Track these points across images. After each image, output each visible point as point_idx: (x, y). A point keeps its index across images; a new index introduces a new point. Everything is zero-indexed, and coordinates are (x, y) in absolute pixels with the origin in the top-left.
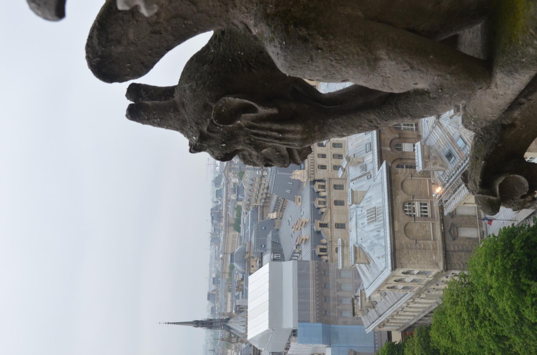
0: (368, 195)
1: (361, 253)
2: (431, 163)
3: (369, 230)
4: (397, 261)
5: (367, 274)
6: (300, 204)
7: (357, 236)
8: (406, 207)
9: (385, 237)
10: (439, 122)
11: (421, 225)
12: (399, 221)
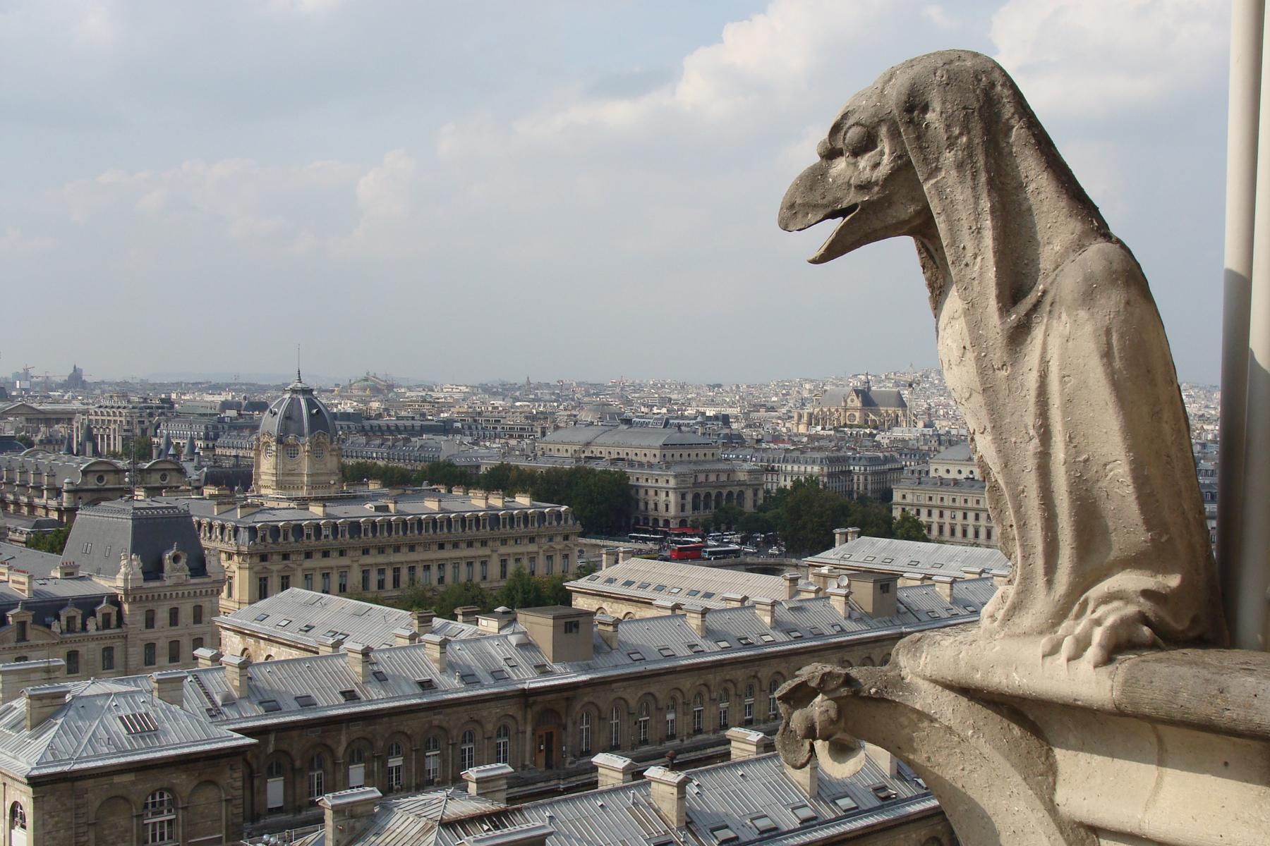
9: (98, 756)
12: (133, 783)
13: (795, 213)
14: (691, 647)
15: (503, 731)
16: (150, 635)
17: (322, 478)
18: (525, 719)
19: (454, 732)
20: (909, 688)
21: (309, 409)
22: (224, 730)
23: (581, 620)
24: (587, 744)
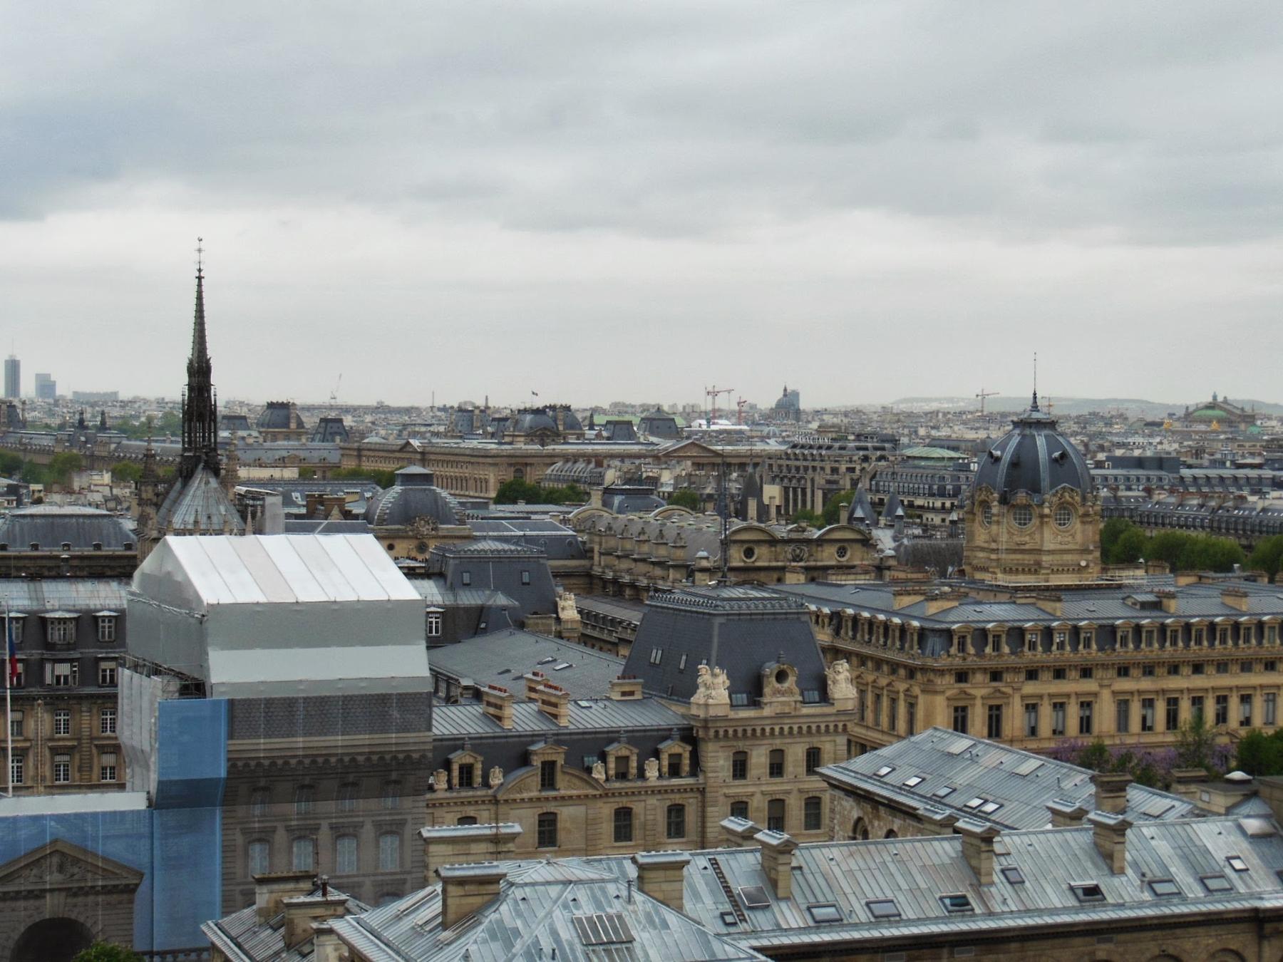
0: (671, 917)
1: (477, 901)
6: (616, 696)
7: (533, 884)
17: (1068, 558)
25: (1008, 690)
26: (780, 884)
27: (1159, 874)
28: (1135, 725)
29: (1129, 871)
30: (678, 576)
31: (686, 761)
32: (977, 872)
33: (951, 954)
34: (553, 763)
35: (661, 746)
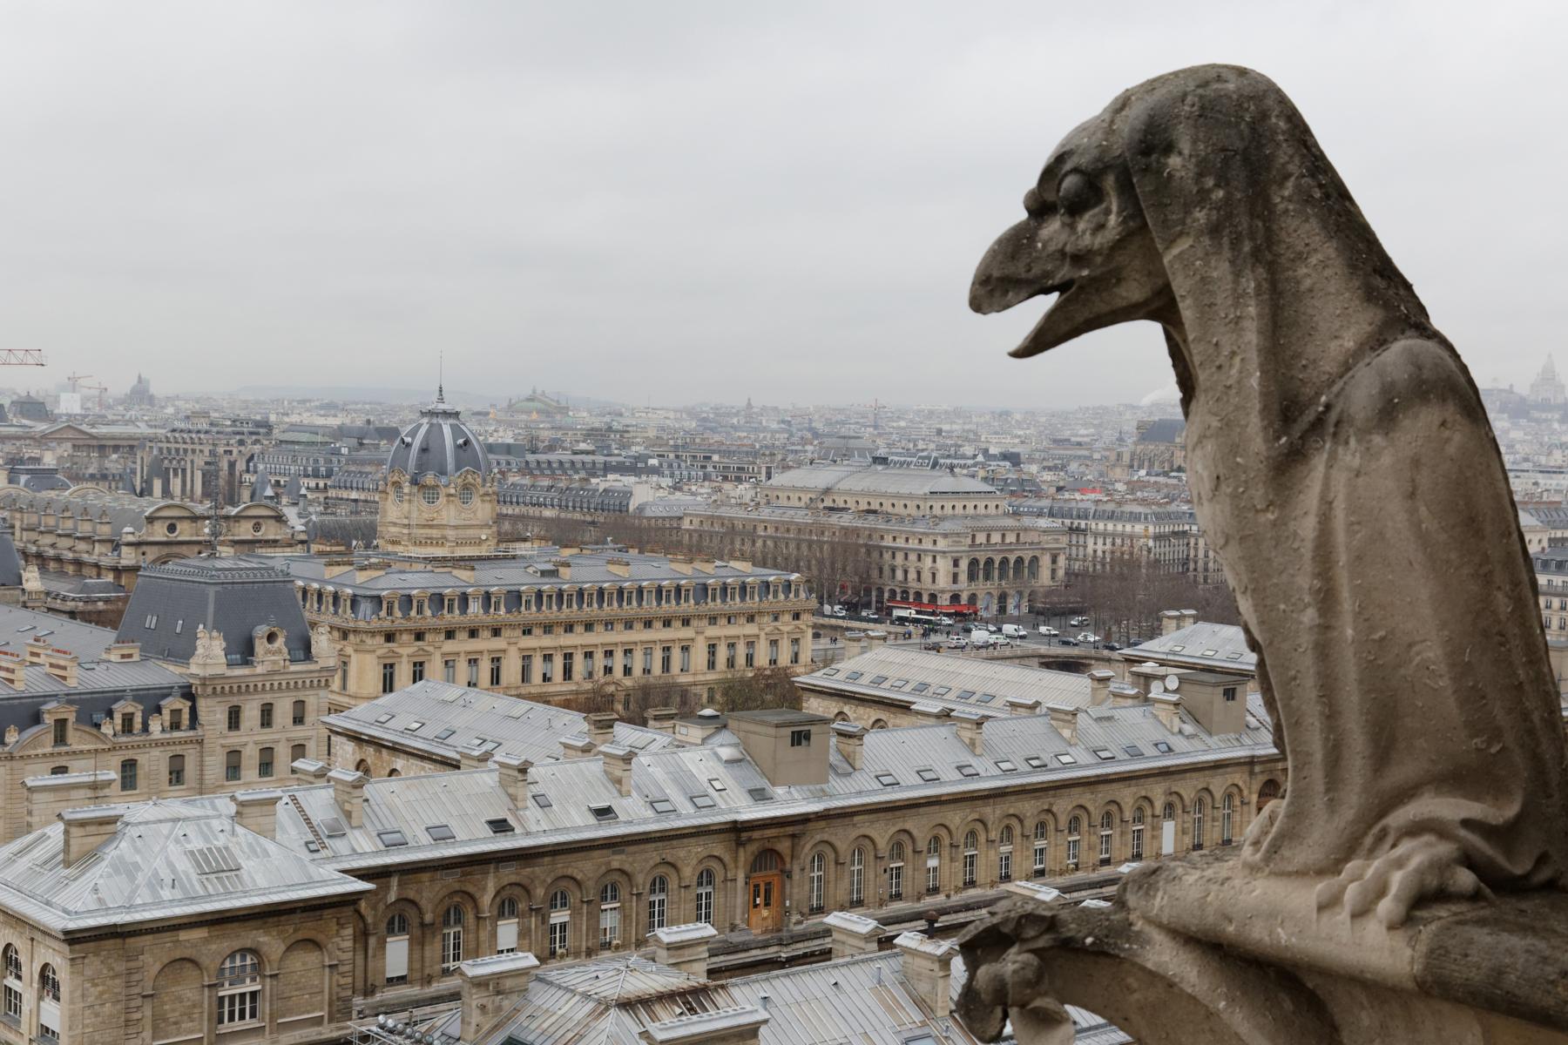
0: (271, 847)
1: (98, 839)
2: (484, 1001)
3: (172, 858)
4: (92, 944)
5: (24, 863)
6: (114, 657)
7: (147, 823)
8: (243, 958)
9: (159, 903)
10: (607, 1009)
11: (194, 1006)
12: (206, 941)
13: (995, 286)
14: (959, 768)
15: (706, 877)
16: (234, 739)
17: (471, 532)
18: (736, 860)
19: (640, 879)
20: (1139, 938)
21: (455, 440)
22: (329, 871)
23: (813, 729)
24: (819, 897)
25: (430, 649)
26: (354, 815)
27: (658, 796)
28: (536, 677)
29: (634, 794)
30: (104, 550)
31: (186, 716)
32: (513, 798)
33: (497, 868)
34: (65, 721)
35: (162, 703)
